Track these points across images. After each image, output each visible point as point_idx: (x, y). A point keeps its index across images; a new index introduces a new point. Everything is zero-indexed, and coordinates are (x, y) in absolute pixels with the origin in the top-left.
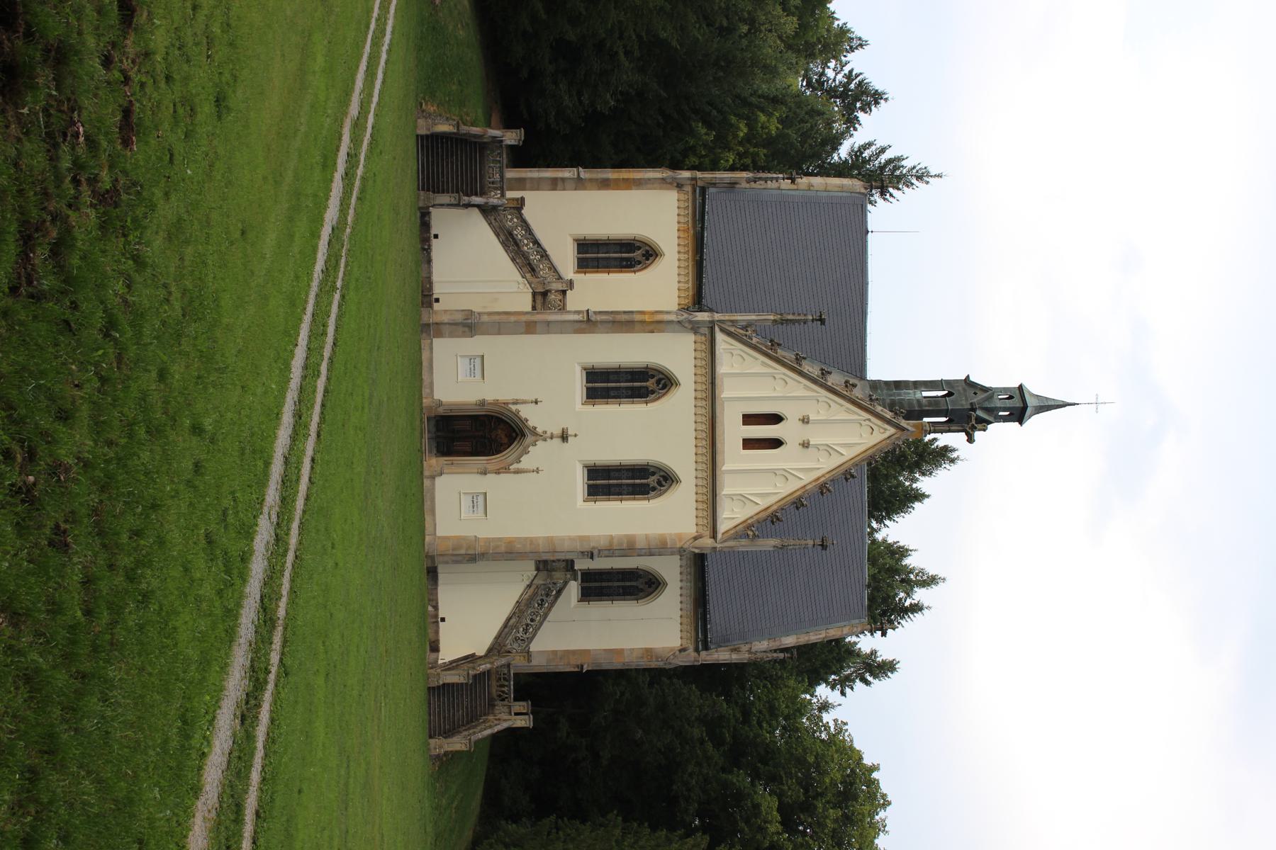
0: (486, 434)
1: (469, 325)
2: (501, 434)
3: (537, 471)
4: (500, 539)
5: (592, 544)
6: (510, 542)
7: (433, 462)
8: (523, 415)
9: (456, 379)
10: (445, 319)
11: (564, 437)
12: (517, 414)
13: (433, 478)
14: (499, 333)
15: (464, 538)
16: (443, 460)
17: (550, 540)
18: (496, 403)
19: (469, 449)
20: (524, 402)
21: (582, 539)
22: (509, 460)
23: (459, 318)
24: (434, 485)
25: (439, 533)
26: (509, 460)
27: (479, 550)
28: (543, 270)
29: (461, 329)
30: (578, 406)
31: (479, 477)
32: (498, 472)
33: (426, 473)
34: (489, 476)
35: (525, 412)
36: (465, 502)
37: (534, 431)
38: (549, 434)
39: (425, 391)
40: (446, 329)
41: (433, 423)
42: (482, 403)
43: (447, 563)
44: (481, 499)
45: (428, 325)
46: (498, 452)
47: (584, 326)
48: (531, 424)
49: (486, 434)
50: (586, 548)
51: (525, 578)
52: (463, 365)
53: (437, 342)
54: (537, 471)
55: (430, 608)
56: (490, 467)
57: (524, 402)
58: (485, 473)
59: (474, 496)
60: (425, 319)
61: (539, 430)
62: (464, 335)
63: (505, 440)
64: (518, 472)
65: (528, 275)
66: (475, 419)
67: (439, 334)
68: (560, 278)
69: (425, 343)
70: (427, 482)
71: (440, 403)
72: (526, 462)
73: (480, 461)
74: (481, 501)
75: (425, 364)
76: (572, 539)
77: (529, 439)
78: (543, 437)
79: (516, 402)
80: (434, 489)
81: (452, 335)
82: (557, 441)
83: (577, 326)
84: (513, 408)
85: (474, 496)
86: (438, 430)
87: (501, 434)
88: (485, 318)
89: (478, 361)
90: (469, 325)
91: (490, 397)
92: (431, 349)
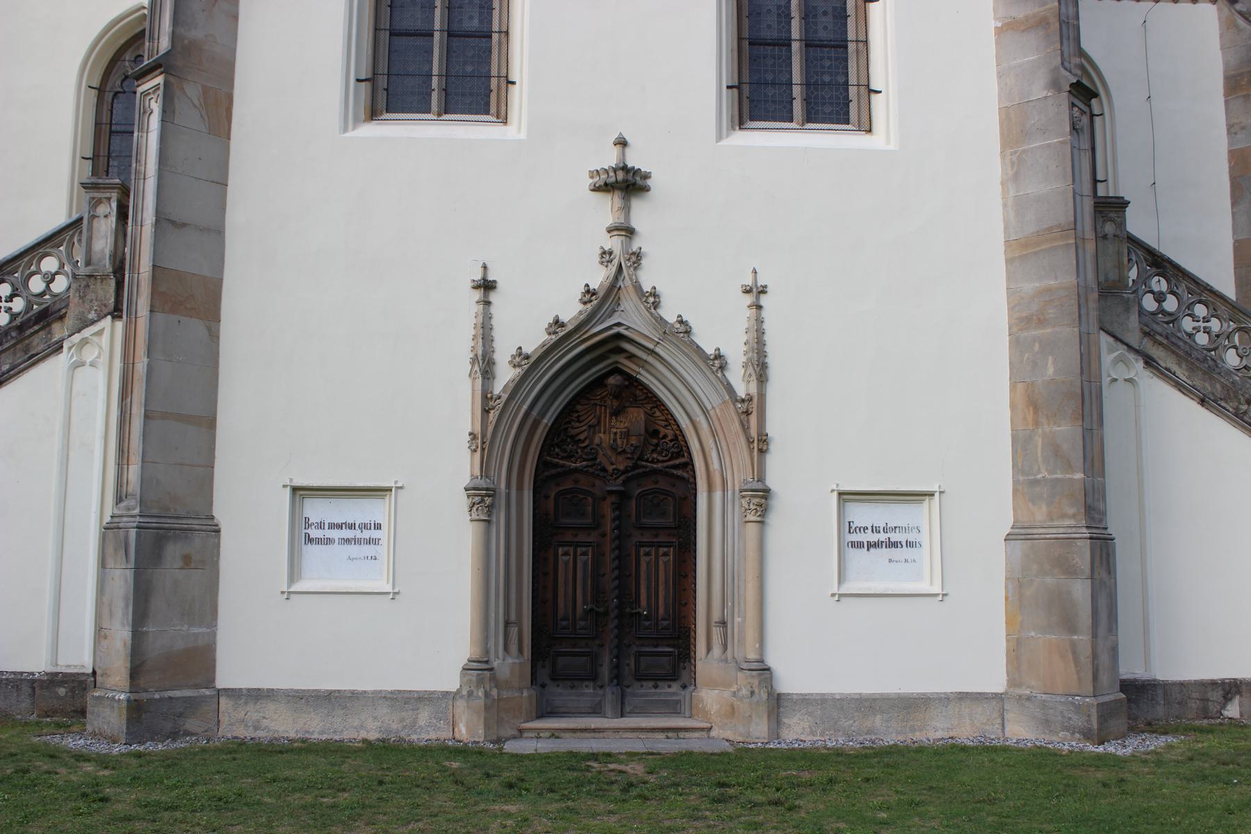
0: (605, 483)
1: (164, 538)
2: (612, 433)
3: (756, 292)
4: (1021, 444)
5: (1039, 91)
6: (1032, 404)
7: (716, 709)
8: (534, 339)
9: (373, 596)
10: (121, 635)
11: (626, 184)
12: (531, 365)
13: (777, 704)
14: (209, 423)
15: (1017, 586)
16: (707, 661)
17: (1021, 252)
18: (483, 443)
19: (666, 560)
20: (485, 332)
21: (1014, 131)
22: (712, 397)
23: (121, 579)
24: (806, 701)
25: (995, 680)
26: (712, 397)
27: (1071, 523)
28: (53, 277)
29: (170, 573)
30: (515, 131)
31: (774, 519)
32: (760, 445)
33: (758, 731)
34: (773, 480)
35: (524, 328)
36: (870, 576)
37: (602, 300)
38: (615, 243)
39: (426, 729)
40: (168, 635)
41: (560, 694)
42: (483, 498)
43: (1114, 651)
44: (862, 514)
45: (136, 710)
46: (680, 448)
47: (193, 91)
48: (571, 310)
49: (605, 483)
50: (1060, 109)
51: (1121, 372)
52: (329, 568)
53: (235, 668)
54: (756, 292)
55: (1233, 710)
56: (739, 472)
57: (485, 332)
58: (762, 497)
59: (852, 540)
60: (108, 717)
61: (598, 277)
62: (205, 561)
63: (636, 417)
64: (760, 368)
65: (58, 331)
66: (546, 535)
67: (200, 661)
68: (76, 224)
69: (235, 724)
70: (798, 731)
71: (480, 668)
72: (721, 331)
73: (714, 514)
74: (871, 515)
75: (315, 727)
76: (1016, 168)
77: (631, 317)
78: (625, 263)
79: (485, 365)
80: (822, 701)
81: (205, 608)
82: (642, 213)
83: (188, 115)
84: (505, 375)
85: (852, 540)
86: (593, 677)
87: (612, 433)
88: (134, 472)
89: (316, 510)
90: (164, 538)
91: (461, 467)
92: (257, 695)
